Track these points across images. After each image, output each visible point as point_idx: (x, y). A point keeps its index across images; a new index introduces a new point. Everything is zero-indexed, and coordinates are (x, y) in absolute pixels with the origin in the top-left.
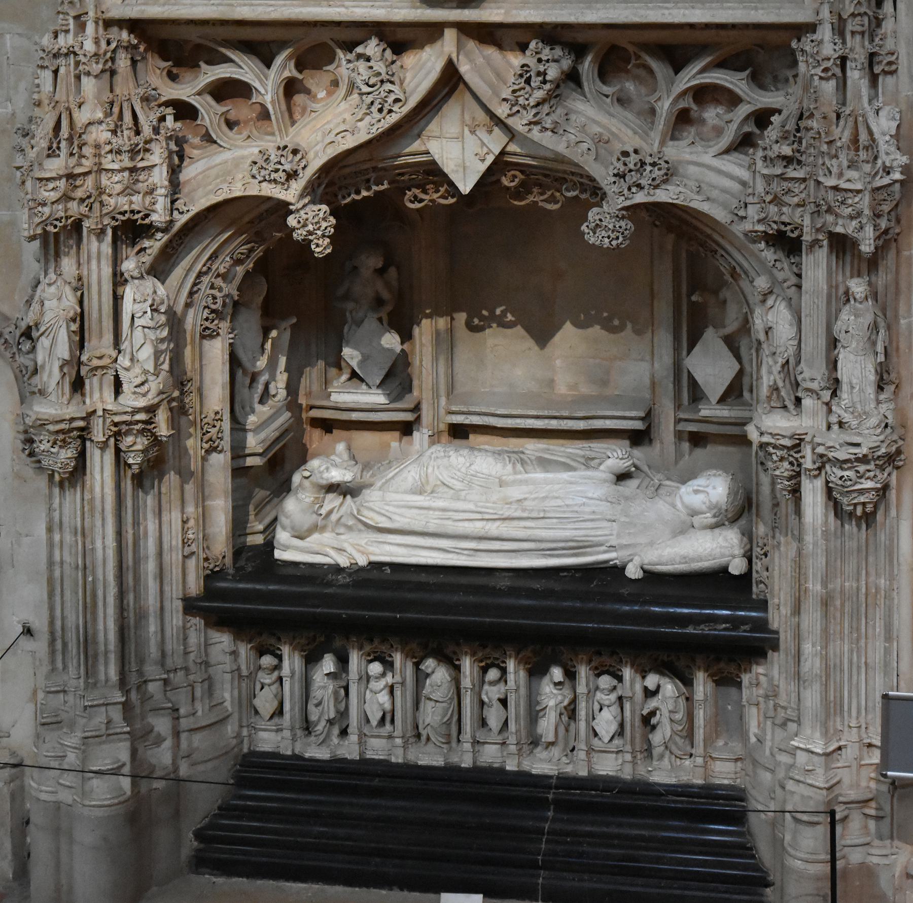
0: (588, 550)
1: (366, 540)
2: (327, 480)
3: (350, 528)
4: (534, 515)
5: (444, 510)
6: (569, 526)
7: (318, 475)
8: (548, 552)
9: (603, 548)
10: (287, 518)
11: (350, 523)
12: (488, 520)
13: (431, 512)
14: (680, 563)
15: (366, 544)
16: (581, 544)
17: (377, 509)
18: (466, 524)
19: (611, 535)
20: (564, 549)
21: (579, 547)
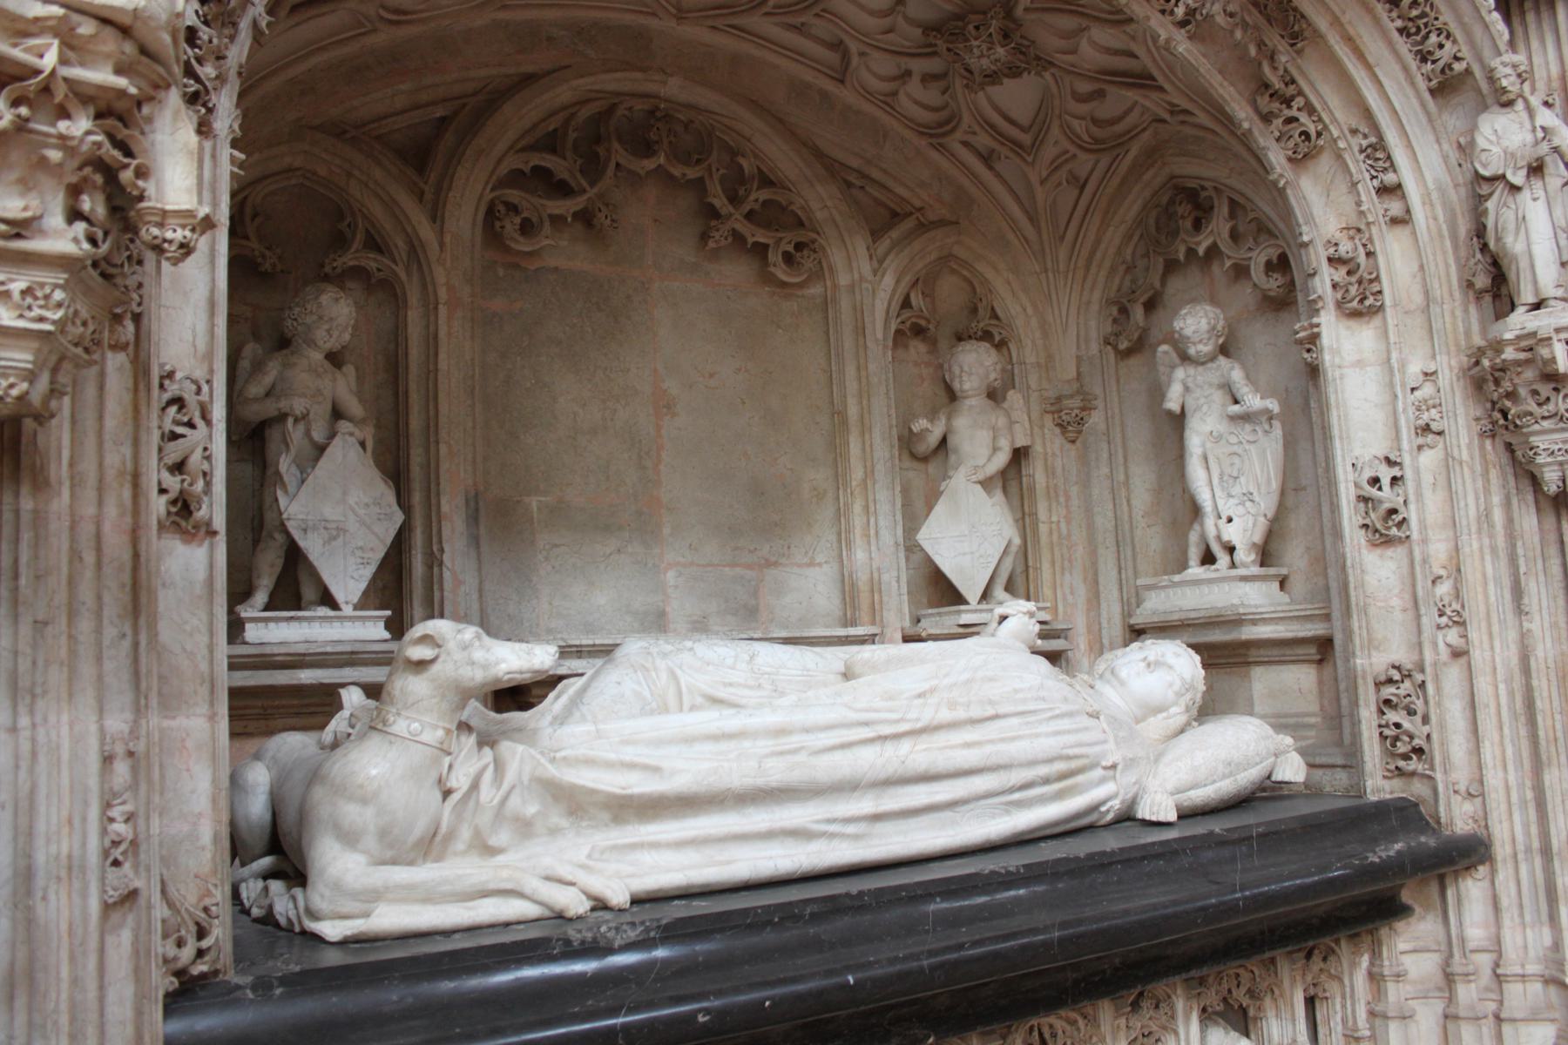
0: (1080, 778)
1: (585, 850)
2: (485, 667)
3: (525, 828)
4: (976, 712)
5: (781, 732)
6: (1043, 728)
7: (458, 656)
8: (1017, 796)
9: (1098, 773)
10: (364, 801)
11: (532, 809)
12: (883, 739)
13: (747, 744)
14: (1224, 777)
15: (589, 856)
16: (1073, 764)
17: (612, 756)
18: (838, 756)
19: (1105, 742)
20: (1046, 781)
21: (1067, 775)
